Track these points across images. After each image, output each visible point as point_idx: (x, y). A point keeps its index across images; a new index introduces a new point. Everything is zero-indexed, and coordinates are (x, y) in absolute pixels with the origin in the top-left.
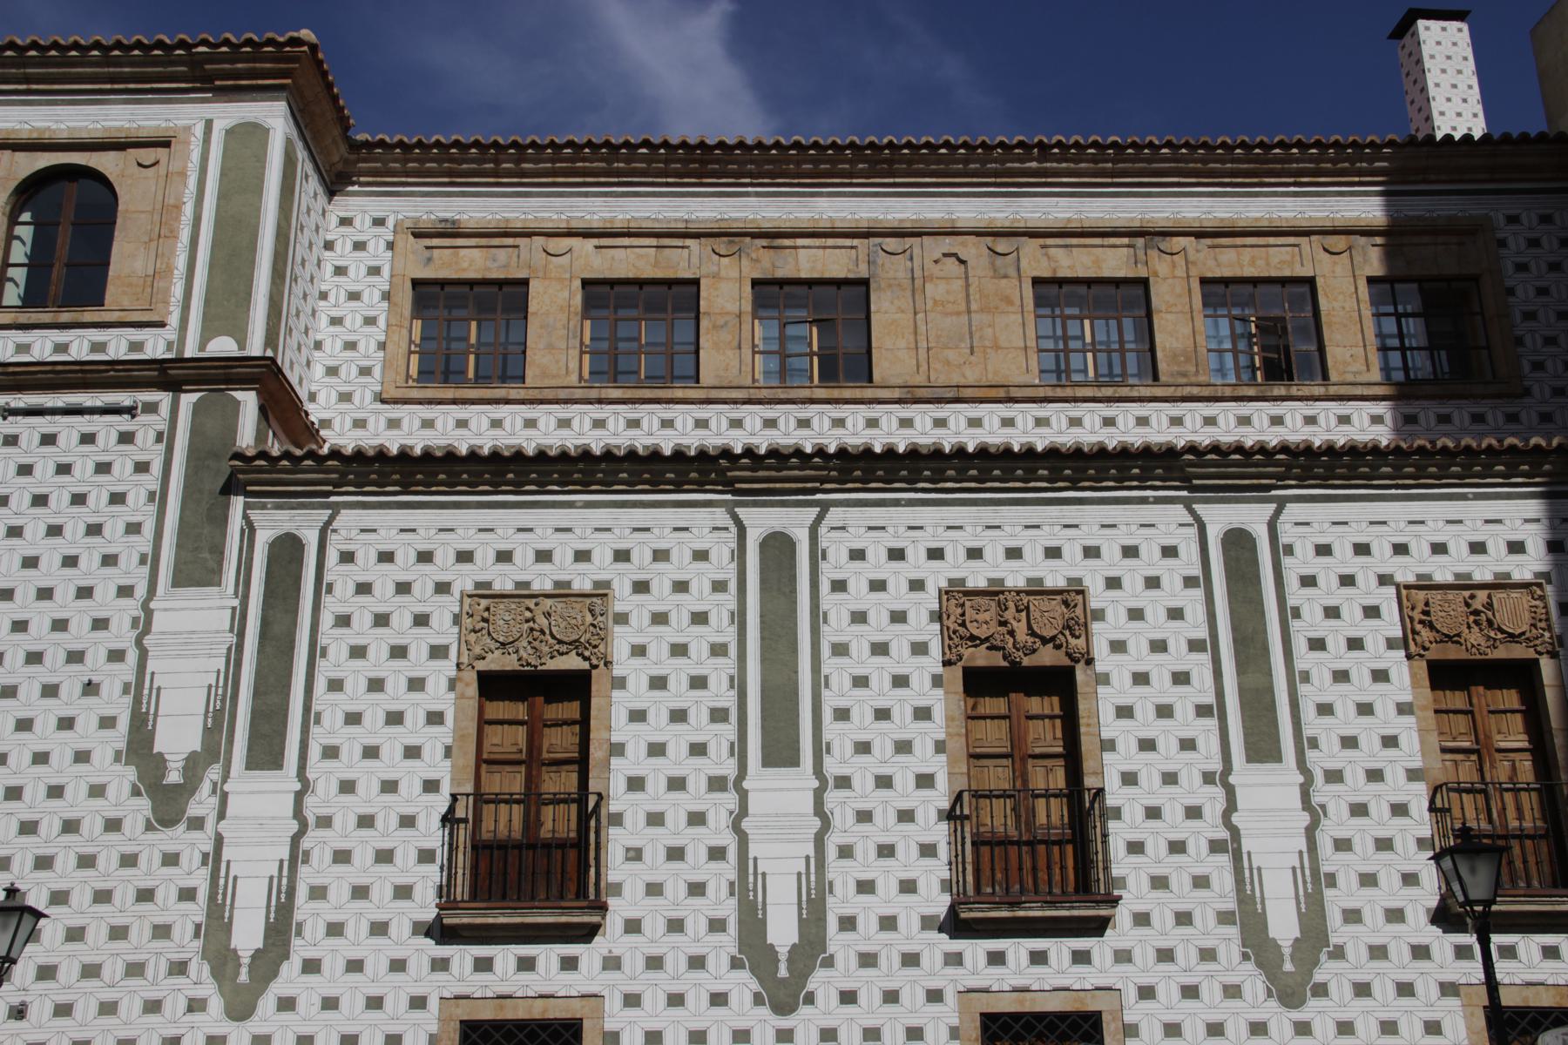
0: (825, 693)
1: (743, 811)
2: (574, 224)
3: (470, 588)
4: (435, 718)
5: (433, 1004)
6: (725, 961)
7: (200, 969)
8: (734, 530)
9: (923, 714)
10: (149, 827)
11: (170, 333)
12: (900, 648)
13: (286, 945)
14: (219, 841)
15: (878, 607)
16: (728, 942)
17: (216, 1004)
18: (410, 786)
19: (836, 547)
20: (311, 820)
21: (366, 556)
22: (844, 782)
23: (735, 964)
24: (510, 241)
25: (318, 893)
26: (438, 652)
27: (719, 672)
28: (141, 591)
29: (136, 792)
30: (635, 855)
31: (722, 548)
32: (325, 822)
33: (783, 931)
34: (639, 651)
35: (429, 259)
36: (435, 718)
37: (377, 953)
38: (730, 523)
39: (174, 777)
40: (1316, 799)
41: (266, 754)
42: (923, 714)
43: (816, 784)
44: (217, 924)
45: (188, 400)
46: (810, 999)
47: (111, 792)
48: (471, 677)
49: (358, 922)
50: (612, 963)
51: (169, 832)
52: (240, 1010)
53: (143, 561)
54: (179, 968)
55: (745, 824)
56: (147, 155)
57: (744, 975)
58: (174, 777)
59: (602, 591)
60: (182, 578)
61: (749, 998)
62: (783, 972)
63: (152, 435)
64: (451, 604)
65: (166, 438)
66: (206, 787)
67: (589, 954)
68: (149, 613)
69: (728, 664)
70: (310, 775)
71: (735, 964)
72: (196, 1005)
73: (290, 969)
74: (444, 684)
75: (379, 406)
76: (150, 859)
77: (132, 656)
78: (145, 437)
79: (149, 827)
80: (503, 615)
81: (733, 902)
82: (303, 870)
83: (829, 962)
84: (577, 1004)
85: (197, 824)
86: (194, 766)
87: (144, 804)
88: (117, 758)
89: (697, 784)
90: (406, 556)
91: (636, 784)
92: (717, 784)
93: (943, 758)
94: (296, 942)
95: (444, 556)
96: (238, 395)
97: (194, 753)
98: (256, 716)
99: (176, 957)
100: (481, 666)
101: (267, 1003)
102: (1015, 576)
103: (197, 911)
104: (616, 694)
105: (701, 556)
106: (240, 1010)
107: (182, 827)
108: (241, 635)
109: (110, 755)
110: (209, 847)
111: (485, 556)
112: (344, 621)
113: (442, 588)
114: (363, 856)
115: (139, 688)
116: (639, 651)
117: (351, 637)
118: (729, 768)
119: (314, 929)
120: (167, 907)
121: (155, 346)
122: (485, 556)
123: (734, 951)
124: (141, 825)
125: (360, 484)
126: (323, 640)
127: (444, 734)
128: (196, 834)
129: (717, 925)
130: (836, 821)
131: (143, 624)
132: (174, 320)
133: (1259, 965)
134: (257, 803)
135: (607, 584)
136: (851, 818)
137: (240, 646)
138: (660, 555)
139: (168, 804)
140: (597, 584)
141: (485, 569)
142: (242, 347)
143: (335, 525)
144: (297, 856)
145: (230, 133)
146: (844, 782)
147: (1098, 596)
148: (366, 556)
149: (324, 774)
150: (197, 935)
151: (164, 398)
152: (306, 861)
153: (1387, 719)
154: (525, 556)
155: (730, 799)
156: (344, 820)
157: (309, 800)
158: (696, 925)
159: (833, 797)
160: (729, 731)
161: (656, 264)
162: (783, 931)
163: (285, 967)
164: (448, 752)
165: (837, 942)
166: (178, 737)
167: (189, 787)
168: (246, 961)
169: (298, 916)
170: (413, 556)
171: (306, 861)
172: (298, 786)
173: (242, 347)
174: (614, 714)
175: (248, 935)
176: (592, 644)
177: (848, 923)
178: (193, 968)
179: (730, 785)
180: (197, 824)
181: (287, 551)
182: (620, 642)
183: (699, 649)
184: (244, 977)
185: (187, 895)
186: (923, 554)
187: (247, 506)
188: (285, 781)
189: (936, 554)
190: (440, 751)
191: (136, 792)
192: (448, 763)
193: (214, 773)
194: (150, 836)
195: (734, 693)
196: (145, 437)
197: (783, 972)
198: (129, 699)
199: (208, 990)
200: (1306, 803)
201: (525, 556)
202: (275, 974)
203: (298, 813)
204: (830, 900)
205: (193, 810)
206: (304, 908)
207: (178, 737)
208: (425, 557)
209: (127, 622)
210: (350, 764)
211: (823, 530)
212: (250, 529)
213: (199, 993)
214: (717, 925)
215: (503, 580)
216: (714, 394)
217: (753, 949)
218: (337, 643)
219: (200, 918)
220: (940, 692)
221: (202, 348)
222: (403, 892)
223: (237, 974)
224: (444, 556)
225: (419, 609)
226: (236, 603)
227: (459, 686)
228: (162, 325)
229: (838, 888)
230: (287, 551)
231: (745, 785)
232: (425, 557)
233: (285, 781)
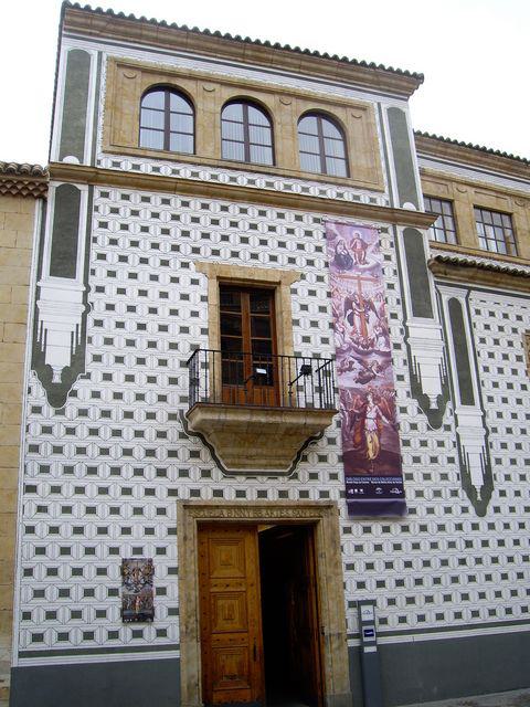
7: (462, 494)
14: (458, 435)
17: (472, 509)
24: (443, 182)
28: (400, 316)
29: (420, 412)
32: (495, 430)
39: (434, 406)
41: (467, 399)
44: (465, 475)
45: (400, 229)
52: (481, 512)
54: (454, 493)
56: (358, 113)
58: (434, 406)
66: (448, 412)
68: (407, 328)
72: (465, 510)
73: (495, 494)
76: (432, 443)
77: (404, 346)
78: (386, 244)
79: (429, 429)
85: (448, 428)
86: (442, 400)
88: (408, 396)
101: (490, 509)
106: (481, 512)
107: (442, 429)
108: (446, 342)
110: (455, 440)
115: (409, 361)
119: (500, 478)
121: (381, 201)
124: (425, 428)
125: (485, 281)
126: (478, 349)
131: (405, 332)
134: (468, 417)
137: (447, 347)
139: (435, 419)
144: (488, 446)
151: (389, 226)
157: (487, 420)
166: (432, 388)
168: (479, 491)
175: (477, 480)
180: (448, 428)
181: (454, 304)
184: (479, 498)
185: (451, 460)
188: (475, 411)
191: (420, 412)
193: (449, 405)
194: (430, 432)
196: (386, 244)
198: (407, 368)
199: (467, 503)
203: (485, 426)
206: (495, 468)
207: (432, 388)
209: (398, 332)
212: (439, 294)
218: (484, 350)
230: (454, 304)
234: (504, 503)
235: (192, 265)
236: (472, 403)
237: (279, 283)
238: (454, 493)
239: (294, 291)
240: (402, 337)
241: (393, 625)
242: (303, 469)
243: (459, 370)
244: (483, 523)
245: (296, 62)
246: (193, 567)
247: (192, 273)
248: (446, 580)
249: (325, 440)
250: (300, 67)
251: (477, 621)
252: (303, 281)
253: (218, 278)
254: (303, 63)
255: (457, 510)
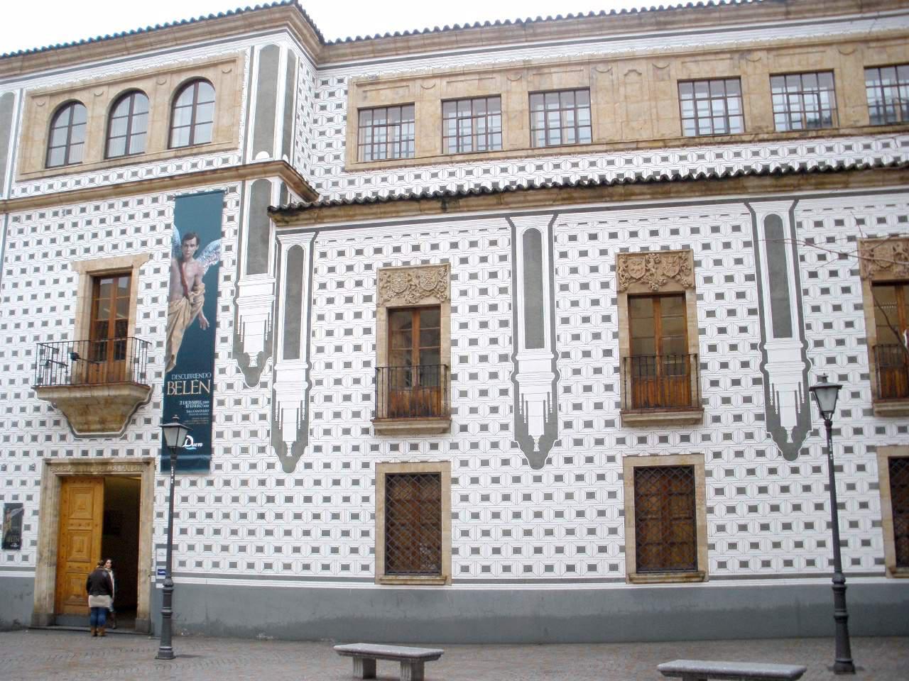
0: (557, 310)
1: (516, 371)
2: (436, 72)
3: (381, 266)
4: (367, 331)
5: (373, 466)
6: (508, 444)
7: (271, 450)
8: (510, 229)
9: (607, 319)
10: (245, 387)
11: (240, 153)
12: (594, 286)
13: (306, 438)
14: (274, 392)
15: (583, 265)
16: (510, 435)
17: (279, 466)
18: (357, 365)
19: (561, 234)
20: (314, 382)
21: (332, 254)
22: (566, 355)
23: (514, 445)
24: (404, 84)
25: (319, 415)
26: (367, 299)
27: (504, 301)
28: (234, 278)
29: (238, 371)
30: (463, 394)
31: (504, 239)
32: (319, 382)
33: (536, 429)
34: (464, 293)
35: (366, 97)
36: (367, 331)
37: (346, 443)
38: (507, 225)
39: (253, 364)
40: (809, 356)
41: (292, 351)
42: (607, 319)
43: (553, 356)
44: (276, 431)
46: (550, 461)
47: (228, 371)
48: (383, 312)
49: (337, 429)
50: (454, 446)
51: (253, 389)
52: (289, 468)
53: (234, 263)
54: (262, 450)
55: (518, 377)
56: (226, 68)
57: (518, 451)
58: (253, 364)
59: (446, 265)
60: (251, 271)
61: (520, 462)
62: (536, 449)
63: (234, 203)
64: (373, 274)
65: (240, 204)
66: (267, 368)
67: (444, 442)
68: (238, 288)
69: (508, 298)
70: (312, 361)
71: (514, 445)
72: (271, 466)
73: (309, 450)
74: (371, 314)
75: (344, 174)
76: (246, 401)
77: (232, 308)
79: (245, 387)
80: (398, 280)
81: (512, 415)
82: (311, 405)
83: (559, 444)
84: (438, 465)
85: (264, 385)
86: (262, 358)
87: (242, 376)
88: (229, 356)
89: (494, 358)
90: (350, 253)
91: (463, 359)
92: (503, 358)
93: (617, 341)
94: (310, 438)
95: (369, 251)
96: (270, 179)
97: (260, 353)
98: (287, 333)
99: (260, 445)
100: (389, 305)
101: (300, 465)
102: (655, 246)
103: (267, 425)
104: (453, 315)
105: (493, 243)
106: (289, 468)
107: (258, 386)
108: (278, 296)
109: (227, 355)
110: (270, 396)
111: (388, 250)
112: (323, 286)
113: (368, 267)
114: (338, 398)
116: (464, 293)
117: (327, 294)
118: (509, 350)
120: (255, 424)
121: (234, 161)
122: (388, 250)
123: (513, 439)
124: (241, 386)
127: (372, 339)
128: (263, 390)
129: (504, 427)
130: (562, 374)
132: (241, 146)
133: (775, 440)
134: (289, 373)
135: (447, 260)
136: (570, 372)
138: (473, 244)
139: (252, 376)
140: (442, 261)
141: (388, 256)
142: (271, 155)
143: (317, 239)
144: (308, 399)
145: (263, 51)
146: (566, 355)
147: (698, 253)
148: (332, 254)
149: (318, 360)
150: (268, 435)
151: (238, 184)
152: (312, 401)
153: (849, 313)
154: (406, 249)
155: (509, 365)
156: (328, 382)
157: (312, 373)
158: (494, 427)
159: (561, 363)
160: (509, 331)
161: (479, 88)
162: (536, 429)
163: (306, 450)
164: (374, 347)
165: (562, 433)
167: (259, 369)
169: (311, 426)
170: (354, 253)
171: (312, 401)
172: (307, 366)
173: (271, 155)
174: (452, 327)
175: (289, 436)
176: (440, 289)
177: (568, 425)
178: (268, 450)
179: (510, 359)
180: (264, 385)
181: (296, 252)
182: (455, 288)
183: (493, 291)
184: (289, 454)
185: (263, 417)
186: (607, 236)
187: (278, 233)
188: (301, 363)
189: (613, 235)
190: (370, 347)
191: (238, 371)
192: (374, 352)
193: (269, 362)
194: (245, 391)
195: (511, 312)
197: (536, 449)
198: (232, 329)
199: (275, 459)
200: (804, 358)
201: (406, 249)
202: (302, 452)
203: (308, 379)
204: (559, 414)
205: (262, 379)
206: (313, 423)
207: (254, 346)
208: (359, 252)
210: (329, 355)
211: (555, 226)
213: (271, 460)
214: (504, 427)
215: (397, 260)
216: (509, 154)
217: (522, 438)
218: (320, 296)
219: (269, 428)
220: (615, 307)
221: (254, 158)
222: (356, 414)
223: (286, 452)
224: (369, 251)
225: (358, 278)
226: (275, 280)
227: (378, 315)
228: (236, 149)
229: (563, 408)
230: (296, 252)
231: (517, 358)
232: (359, 252)
233: (301, 363)
234: (317, 460)
235: (69, 266)
236: (295, 355)
237: (132, 267)
238: (262, 450)
239: (142, 272)
240: (232, 298)
241: (190, 568)
242: (132, 431)
243: (287, 323)
244: (289, 479)
245: (170, 36)
246: (50, 510)
247: (69, 272)
248: (243, 532)
249: (151, 404)
250: (176, 39)
251: (269, 572)
252: (152, 261)
253: (88, 272)
254: (177, 35)
255: (262, 466)
